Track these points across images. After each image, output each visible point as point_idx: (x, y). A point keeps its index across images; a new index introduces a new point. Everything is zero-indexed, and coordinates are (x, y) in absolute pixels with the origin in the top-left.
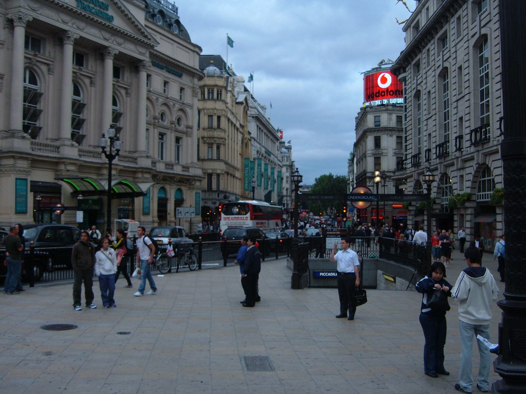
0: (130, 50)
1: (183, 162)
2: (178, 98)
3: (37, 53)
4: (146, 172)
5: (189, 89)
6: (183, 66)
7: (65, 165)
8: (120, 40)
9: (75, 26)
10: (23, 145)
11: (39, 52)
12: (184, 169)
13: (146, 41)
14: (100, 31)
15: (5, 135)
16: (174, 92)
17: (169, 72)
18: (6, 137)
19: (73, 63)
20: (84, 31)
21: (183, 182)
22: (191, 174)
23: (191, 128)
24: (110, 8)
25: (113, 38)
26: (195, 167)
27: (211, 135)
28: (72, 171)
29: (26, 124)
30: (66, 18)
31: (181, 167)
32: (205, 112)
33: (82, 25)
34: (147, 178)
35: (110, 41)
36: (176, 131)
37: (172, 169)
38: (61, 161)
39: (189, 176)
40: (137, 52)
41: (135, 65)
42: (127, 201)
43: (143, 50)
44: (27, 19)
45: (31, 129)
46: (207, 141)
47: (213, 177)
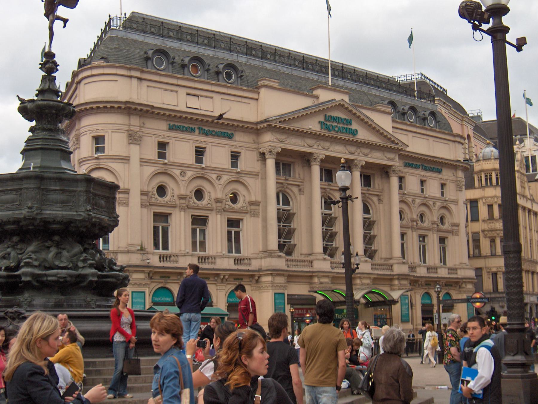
0: (378, 158)
1: (450, 263)
2: (438, 195)
3: (288, 178)
4: (403, 279)
5: (451, 183)
6: (441, 160)
7: (318, 277)
8: (366, 151)
9: (320, 147)
10: (280, 263)
11: (290, 176)
12: (451, 271)
13: (393, 146)
14: (346, 147)
15: (263, 256)
16: (433, 189)
17: (426, 170)
18: (265, 257)
19: (321, 180)
20: (330, 150)
21: (451, 285)
22: (459, 277)
23: (457, 225)
24: (353, 122)
25: (359, 151)
26: (464, 269)
27: (493, 227)
28: (325, 283)
29: (282, 242)
30: (311, 141)
31: (447, 270)
32: (484, 201)
33: (327, 144)
34: (405, 285)
35: (356, 154)
36: (439, 231)
37: (436, 273)
38: (314, 274)
39: (457, 278)
40: (386, 159)
41: (385, 171)
42: (386, 308)
43: (392, 156)
44: (276, 151)
45: (286, 247)
46: (489, 235)
47: (498, 276)
